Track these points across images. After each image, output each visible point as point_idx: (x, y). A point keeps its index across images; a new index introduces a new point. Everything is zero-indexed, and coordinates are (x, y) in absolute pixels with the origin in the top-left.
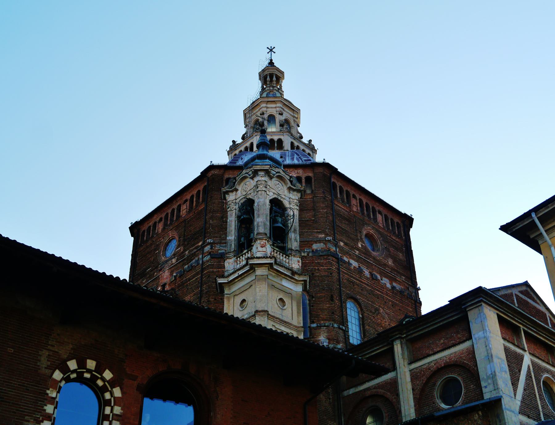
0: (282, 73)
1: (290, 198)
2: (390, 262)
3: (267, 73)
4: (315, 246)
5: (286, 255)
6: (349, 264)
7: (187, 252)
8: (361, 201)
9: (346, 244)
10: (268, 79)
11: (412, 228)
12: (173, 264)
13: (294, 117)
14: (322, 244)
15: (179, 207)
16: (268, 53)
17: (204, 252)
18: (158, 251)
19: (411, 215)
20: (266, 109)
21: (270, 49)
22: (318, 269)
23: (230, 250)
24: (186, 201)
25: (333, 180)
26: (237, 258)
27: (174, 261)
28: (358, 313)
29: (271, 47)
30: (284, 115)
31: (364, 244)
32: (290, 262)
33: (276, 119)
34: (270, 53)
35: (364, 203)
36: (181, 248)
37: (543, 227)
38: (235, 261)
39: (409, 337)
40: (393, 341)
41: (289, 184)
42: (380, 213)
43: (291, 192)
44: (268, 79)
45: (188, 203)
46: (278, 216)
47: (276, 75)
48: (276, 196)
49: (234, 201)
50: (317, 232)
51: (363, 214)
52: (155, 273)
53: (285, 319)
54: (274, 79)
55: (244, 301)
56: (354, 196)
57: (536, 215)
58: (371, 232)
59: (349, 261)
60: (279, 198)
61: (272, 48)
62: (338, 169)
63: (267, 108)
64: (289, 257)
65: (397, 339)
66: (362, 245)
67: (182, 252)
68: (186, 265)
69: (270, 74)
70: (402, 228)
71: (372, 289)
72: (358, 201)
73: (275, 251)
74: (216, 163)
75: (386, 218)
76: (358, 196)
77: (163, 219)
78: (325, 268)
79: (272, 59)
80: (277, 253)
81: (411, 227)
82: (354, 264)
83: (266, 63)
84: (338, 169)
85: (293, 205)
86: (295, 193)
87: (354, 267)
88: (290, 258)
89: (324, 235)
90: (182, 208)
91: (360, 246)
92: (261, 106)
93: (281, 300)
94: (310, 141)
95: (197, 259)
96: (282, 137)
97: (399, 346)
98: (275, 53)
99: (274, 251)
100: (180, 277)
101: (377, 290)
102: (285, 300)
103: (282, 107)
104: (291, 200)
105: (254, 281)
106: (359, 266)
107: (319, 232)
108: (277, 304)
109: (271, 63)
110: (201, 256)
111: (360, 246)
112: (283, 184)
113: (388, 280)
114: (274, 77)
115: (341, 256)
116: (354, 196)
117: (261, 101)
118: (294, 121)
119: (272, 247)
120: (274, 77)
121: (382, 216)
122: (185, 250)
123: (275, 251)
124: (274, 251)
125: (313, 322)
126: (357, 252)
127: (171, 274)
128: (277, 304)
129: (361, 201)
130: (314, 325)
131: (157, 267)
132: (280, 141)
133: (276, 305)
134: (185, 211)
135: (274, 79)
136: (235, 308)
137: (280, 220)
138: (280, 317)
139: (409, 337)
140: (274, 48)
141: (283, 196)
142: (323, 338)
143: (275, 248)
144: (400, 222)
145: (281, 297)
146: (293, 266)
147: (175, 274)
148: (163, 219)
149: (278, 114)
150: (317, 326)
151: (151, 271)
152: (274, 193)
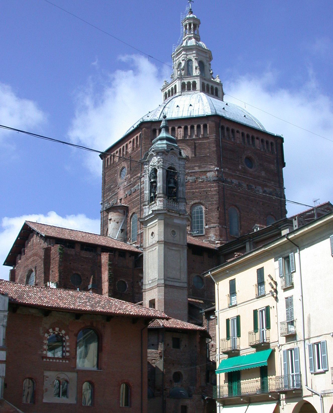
1: (179, 164)
2: (263, 174)
3: (187, 23)
4: (209, 174)
5: (177, 203)
6: (232, 182)
7: (132, 179)
8: (243, 134)
9: (230, 169)
10: (188, 27)
11: (283, 142)
12: (125, 186)
13: (206, 57)
14: (213, 172)
15: (127, 145)
17: (141, 181)
18: (116, 175)
22: (210, 190)
23: (146, 200)
24: (130, 142)
25: (221, 124)
26: (150, 206)
27: (125, 183)
31: (244, 165)
32: (179, 206)
35: (246, 135)
36: (129, 176)
37: (213, 277)
38: (148, 207)
39: (254, 241)
40: (245, 243)
41: (179, 156)
42: (257, 138)
43: (180, 160)
44: (188, 27)
45: (132, 143)
46: (172, 179)
48: (170, 165)
49: (147, 168)
50: (210, 164)
51: (244, 142)
52: (116, 190)
53: (175, 242)
55: (153, 233)
56: (238, 132)
57: (211, 273)
58: (249, 155)
59: (231, 181)
60: (173, 166)
64: (178, 203)
65: (248, 241)
66: (242, 167)
67: (130, 179)
68: (132, 188)
69: (189, 23)
70: (275, 146)
71: (248, 196)
72: (241, 135)
73: (170, 202)
75: (262, 141)
76: (241, 131)
77: (118, 152)
78: (215, 189)
80: (171, 202)
81: (283, 142)
82: (235, 181)
85: (182, 168)
86: (183, 160)
87: (235, 184)
88: (179, 204)
89: (214, 166)
90: (128, 146)
91: (240, 167)
93: (173, 231)
95: (137, 185)
97: (248, 245)
99: (169, 202)
100: (129, 195)
101: (252, 196)
102: (175, 231)
104: (180, 165)
105: (157, 222)
106: (239, 183)
107: (211, 164)
108: (171, 234)
110: (139, 184)
111: (240, 167)
112: (175, 155)
113: (261, 187)
115: (226, 179)
116: (238, 132)
118: (207, 61)
119: (168, 200)
121: (259, 140)
122: (131, 178)
123: (170, 202)
124: (169, 202)
125: (206, 225)
126: (238, 172)
127: (125, 192)
128: (171, 234)
129: (243, 134)
130: (207, 227)
131: (116, 186)
132: (194, 83)
133: (170, 235)
134: (130, 149)
136: (149, 236)
137: (172, 181)
138: (172, 242)
139: (254, 241)
141: (175, 164)
142: (213, 235)
143: (169, 200)
144: (273, 142)
145: (173, 230)
146: (181, 208)
147: (126, 193)
148: (118, 152)
149: (194, 59)
150: (209, 227)
151: (114, 187)
152: (169, 164)
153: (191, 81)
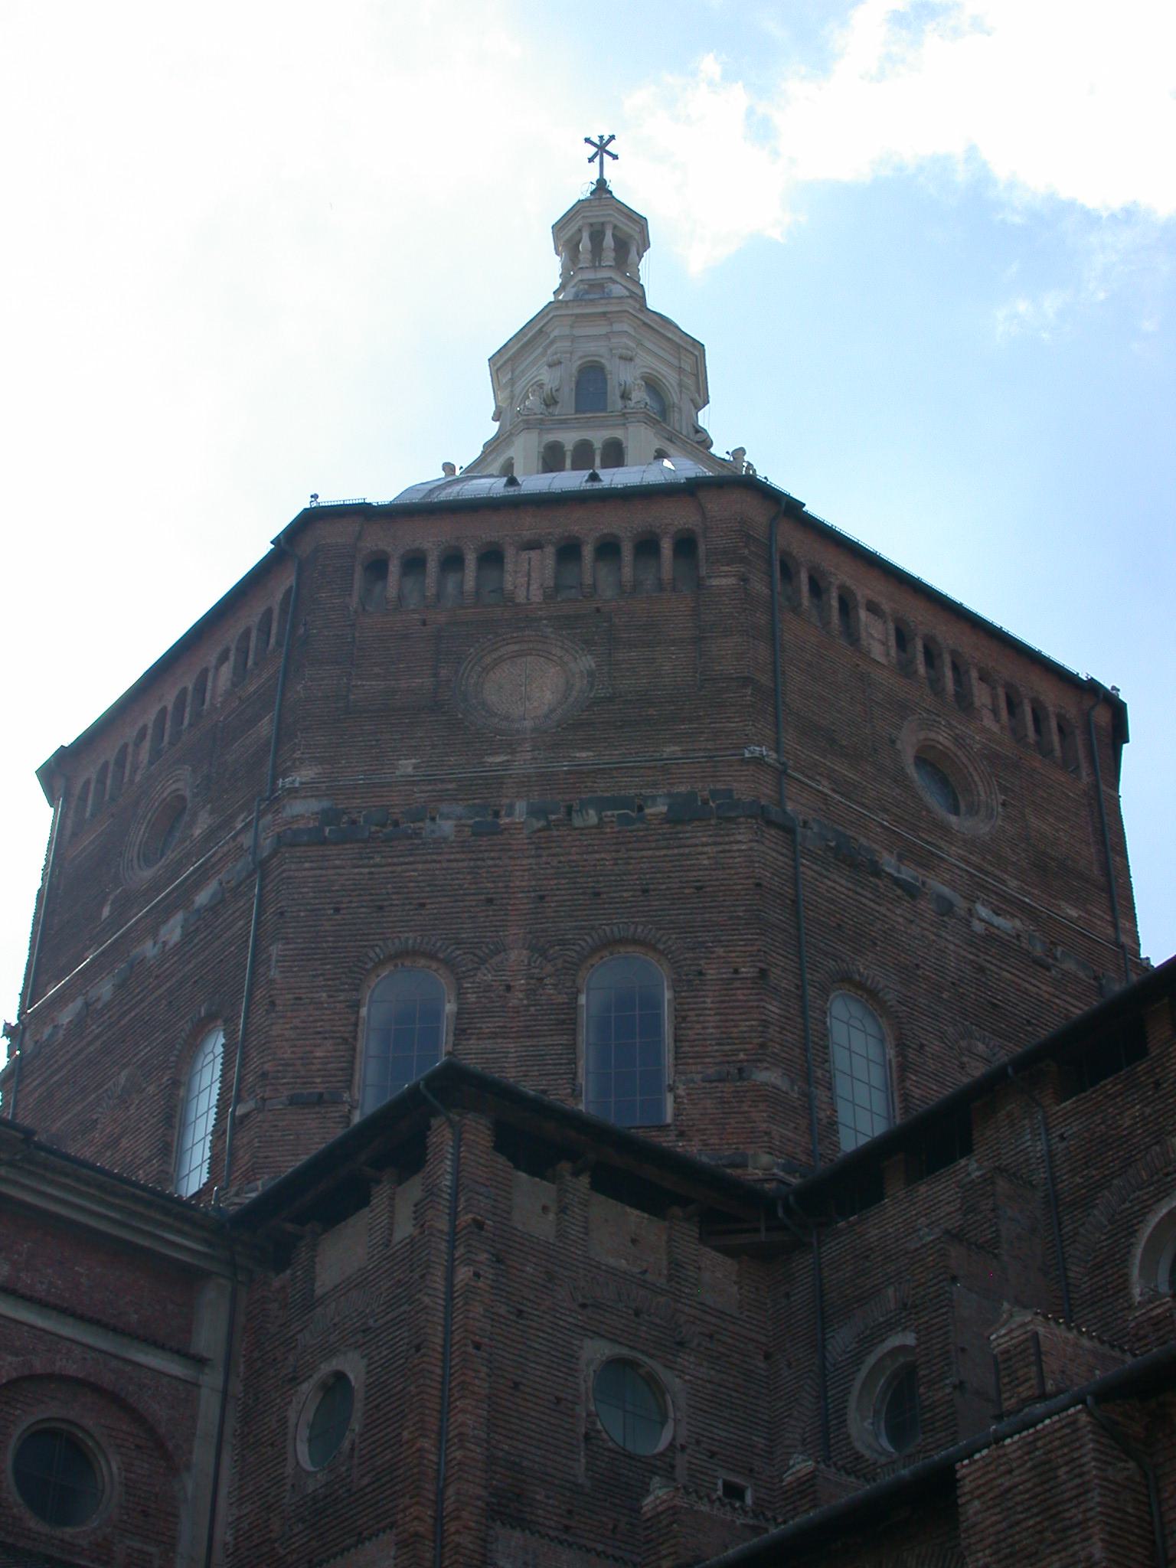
0: (640, 222)
11: (1127, 741)
16: (591, 160)
19: (1114, 688)
20: (569, 344)
21: (598, 143)
28: (882, 1041)
29: (601, 137)
30: (637, 360)
33: (609, 377)
34: (597, 159)
44: (585, 245)
47: (615, 227)
54: (609, 241)
61: (606, 138)
62: (804, 505)
63: (574, 339)
72: (891, 626)
74: (327, 499)
79: (606, 177)
83: (582, 189)
84: (804, 505)
92: (552, 336)
94: (740, 452)
96: (618, 434)
98: (615, 157)
103: (631, 331)
109: (601, 185)
114: (609, 233)
117: (554, 316)
120: (609, 233)
135: (609, 241)
140: (612, 137)
153: (598, 437)
